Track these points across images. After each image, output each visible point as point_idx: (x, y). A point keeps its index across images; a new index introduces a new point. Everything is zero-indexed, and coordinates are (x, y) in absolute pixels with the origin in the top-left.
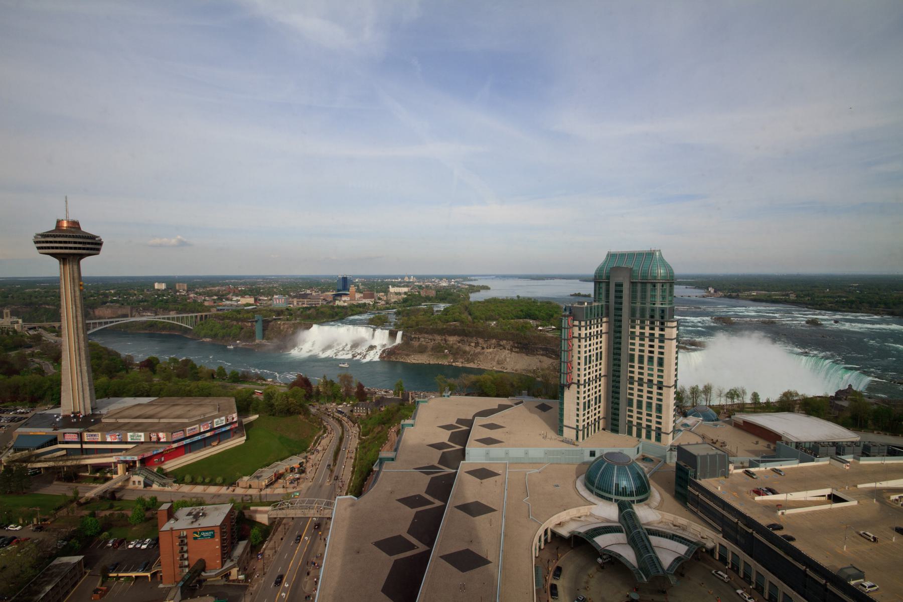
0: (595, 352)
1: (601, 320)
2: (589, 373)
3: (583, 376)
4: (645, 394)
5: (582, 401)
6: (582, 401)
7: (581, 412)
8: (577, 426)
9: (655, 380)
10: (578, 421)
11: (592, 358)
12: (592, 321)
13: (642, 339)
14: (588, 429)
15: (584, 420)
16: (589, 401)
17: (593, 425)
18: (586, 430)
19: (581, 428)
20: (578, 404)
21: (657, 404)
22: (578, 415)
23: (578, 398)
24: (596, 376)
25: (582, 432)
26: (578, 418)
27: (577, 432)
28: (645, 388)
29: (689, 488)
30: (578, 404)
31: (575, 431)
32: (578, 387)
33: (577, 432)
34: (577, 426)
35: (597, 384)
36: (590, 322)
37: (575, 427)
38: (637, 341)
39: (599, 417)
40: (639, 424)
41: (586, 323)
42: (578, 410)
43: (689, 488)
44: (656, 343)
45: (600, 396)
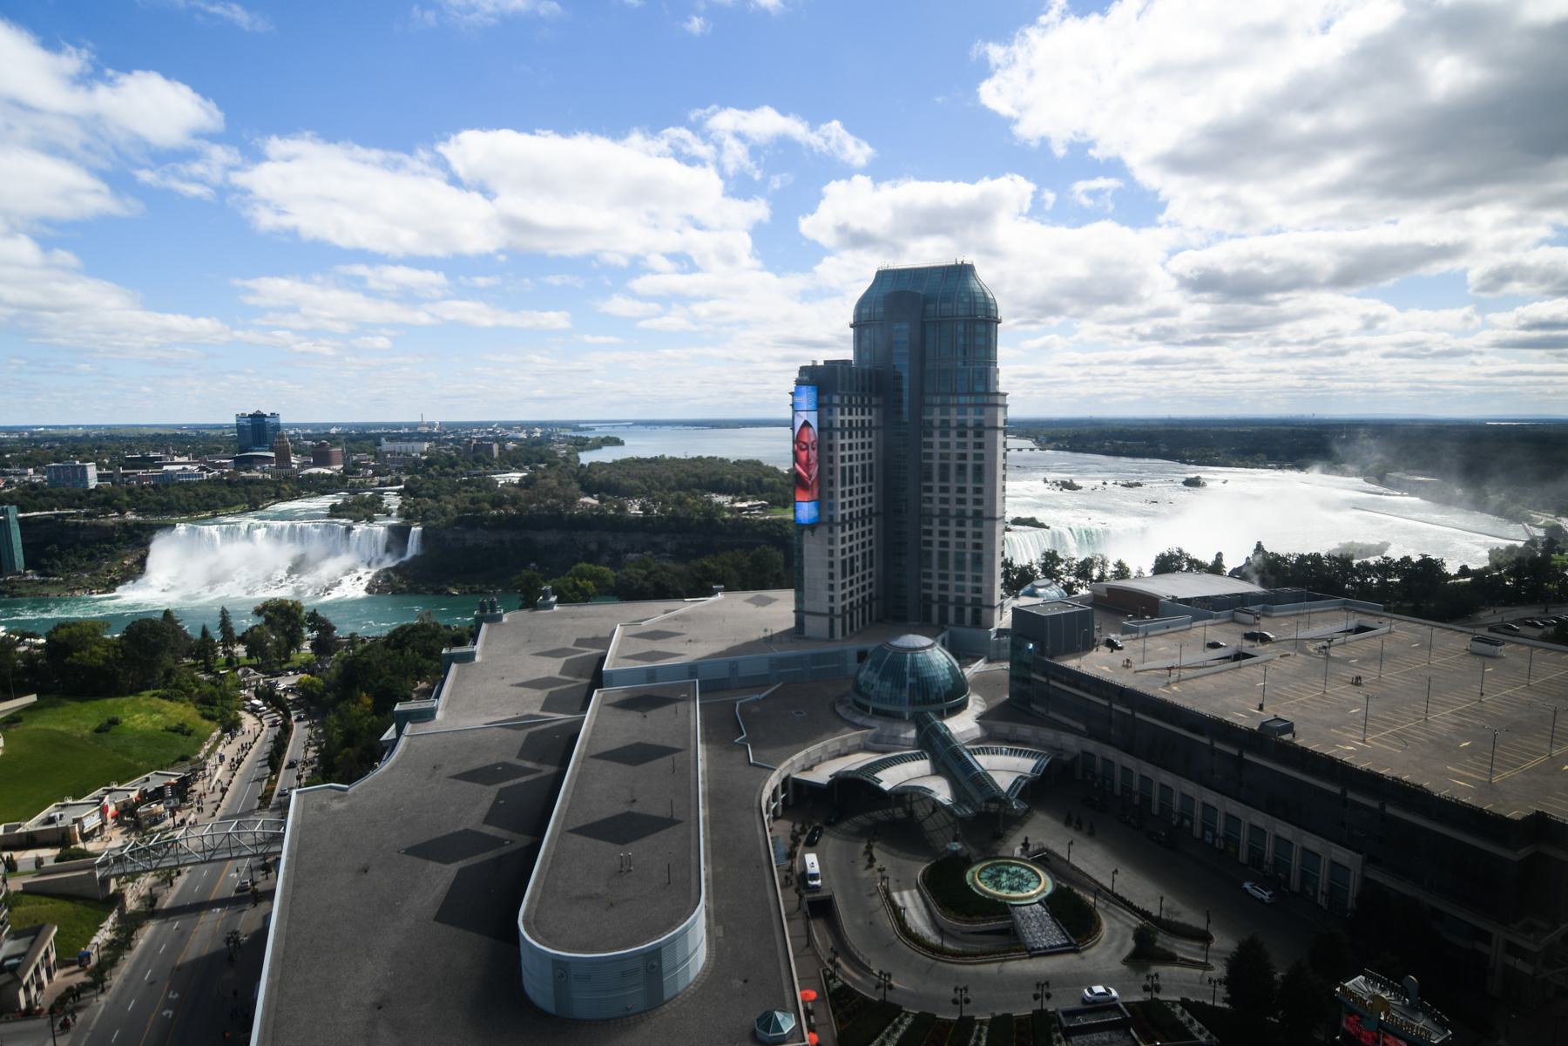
0: (860, 463)
1: (870, 401)
2: (851, 504)
3: (839, 508)
4: (953, 540)
5: (838, 557)
6: (838, 557)
7: (838, 581)
8: (832, 609)
9: (970, 508)
10: (832, 599)
11: (856, 475)
12: (854, 398)
13: (945, 434)
14: (851, 617)
15: (844, 597)
16: (852, 559)
17: (860, 610)
18: (848, 616)
19: (838, 611)
20: (831, 565)
21: (973, 554)
22: (831, 587)
23: (831, 553)
24: (863, 511)
25: (840, 620)
26: (831, 593)
27: (832, 622)
28: (953, 527)
29: (1033, 706)
30: (831, 565)
31: (826, 620)
32: (831, 531)
33: (832, 622)
34: (832, 609)
35: (866, 528)
36: (850, 401)
37: (827, 611)
38: (936, 439)
39: (870, 595)
40: (944, 599)
41: (842, 400)
42: (831, 576)
43: (1033, 706)
44: (970, 438)
45: (871, 552)
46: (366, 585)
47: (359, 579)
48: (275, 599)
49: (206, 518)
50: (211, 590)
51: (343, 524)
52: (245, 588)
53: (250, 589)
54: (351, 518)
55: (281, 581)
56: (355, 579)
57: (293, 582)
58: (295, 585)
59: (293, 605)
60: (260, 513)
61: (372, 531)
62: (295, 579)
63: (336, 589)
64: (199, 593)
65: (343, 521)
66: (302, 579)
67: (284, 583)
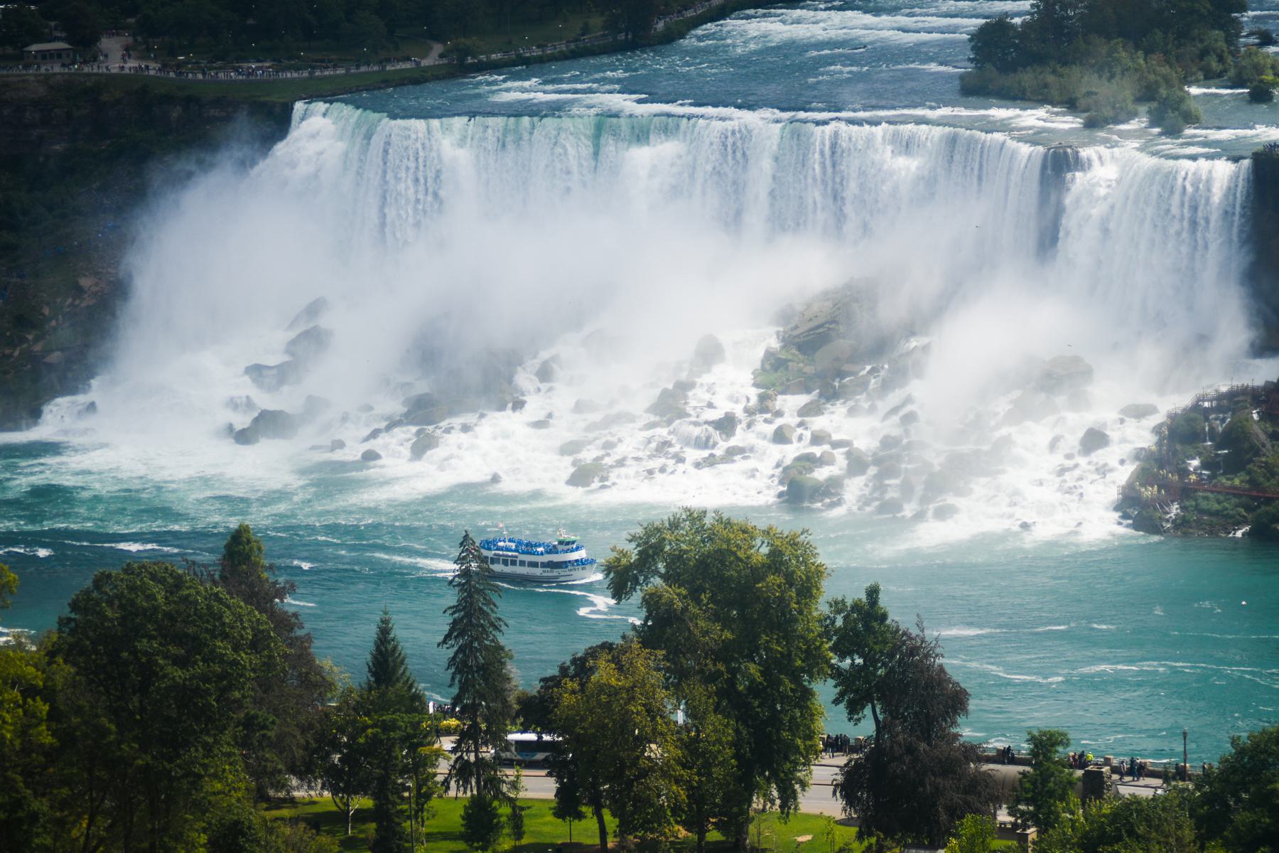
46: (1124, 474)
47: (1095, 439)
48: (695, 517)
49: (418, 79)
50: (421, 447)
51: (1034, 138)
52: (568, 449)
53: (588, 455)
54: (1071, 105)
55: (726, 425)
56: (1073, 440)
57: (781, 437)
58: (791, 452)
59: (775, 554)
60: (651, 62)
61: (1170, 176)
62: (790, 419)
63: (980, 486)
64: (370, 456)
65: (1034, 117)
66: (819, 423)
67: (740, 438)
